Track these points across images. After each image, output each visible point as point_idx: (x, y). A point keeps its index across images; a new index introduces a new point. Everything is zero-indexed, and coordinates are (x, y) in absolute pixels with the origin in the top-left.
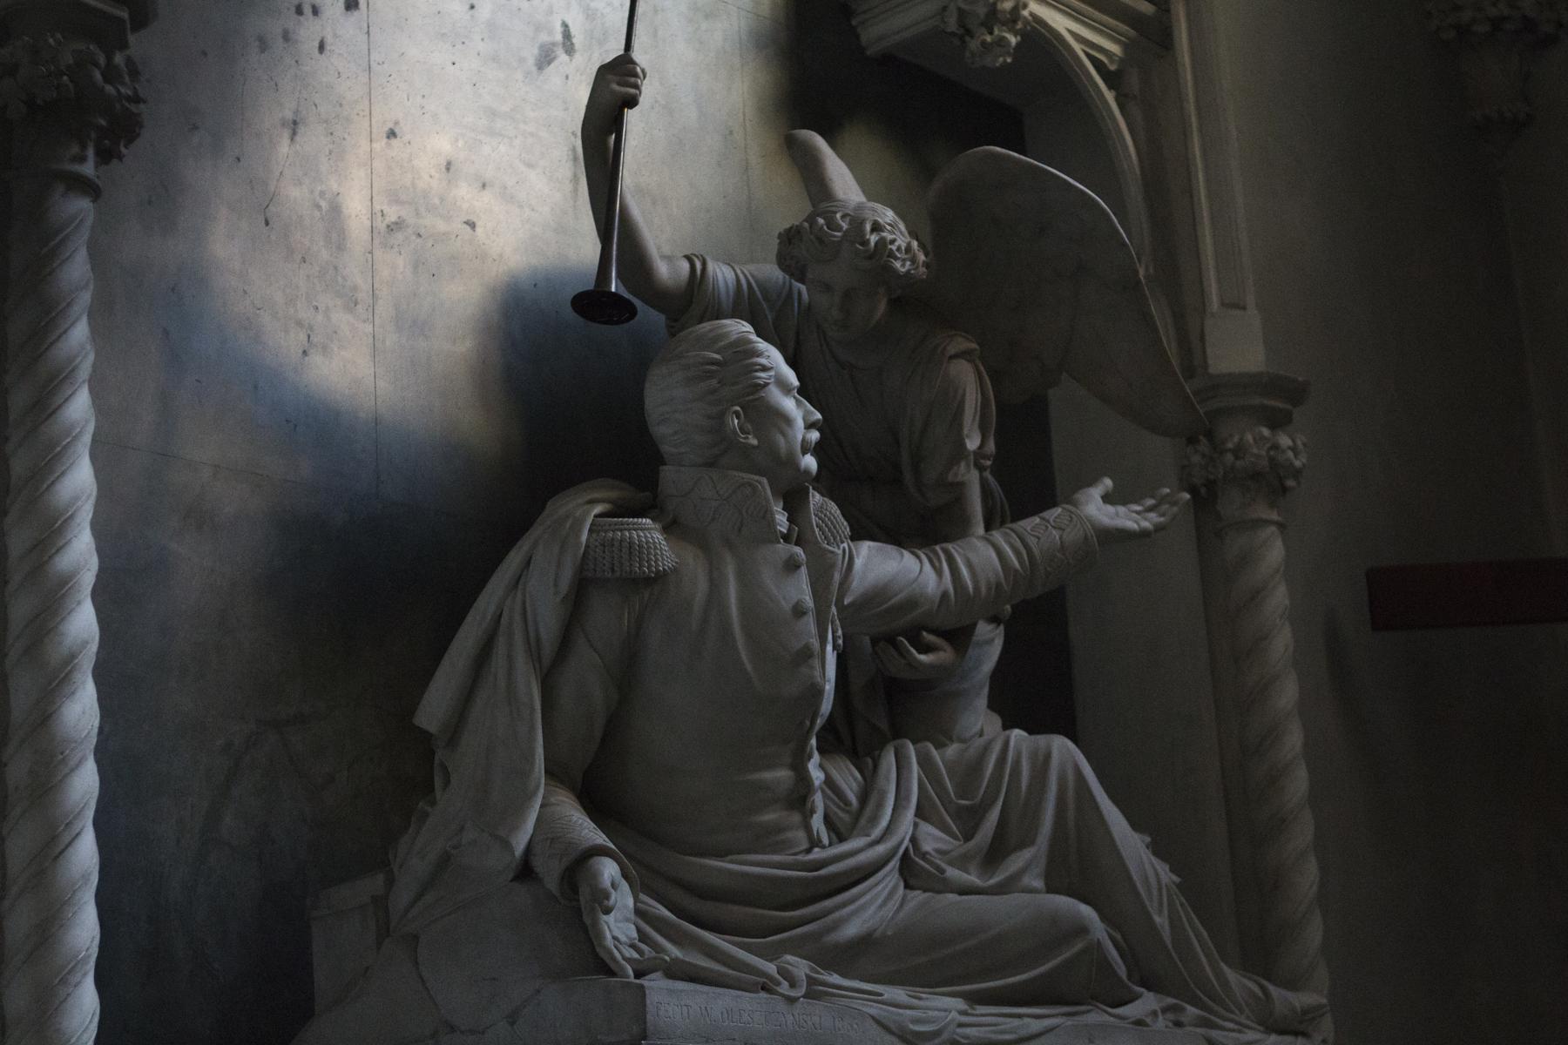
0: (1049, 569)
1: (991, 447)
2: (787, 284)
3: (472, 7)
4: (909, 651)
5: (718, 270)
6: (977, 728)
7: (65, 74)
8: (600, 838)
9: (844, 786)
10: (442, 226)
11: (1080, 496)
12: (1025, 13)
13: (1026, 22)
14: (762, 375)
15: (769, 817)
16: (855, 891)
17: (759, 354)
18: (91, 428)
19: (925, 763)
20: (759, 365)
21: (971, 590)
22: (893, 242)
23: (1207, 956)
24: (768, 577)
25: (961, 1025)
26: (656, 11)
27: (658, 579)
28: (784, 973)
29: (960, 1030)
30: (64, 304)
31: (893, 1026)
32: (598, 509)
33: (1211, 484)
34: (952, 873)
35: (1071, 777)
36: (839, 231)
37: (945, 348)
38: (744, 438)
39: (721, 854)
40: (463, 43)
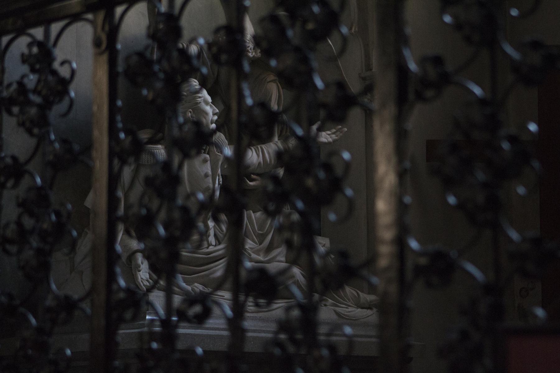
14: (199, 99)
20: (198, 96)
21: (268, 160)
37: (266, 79)
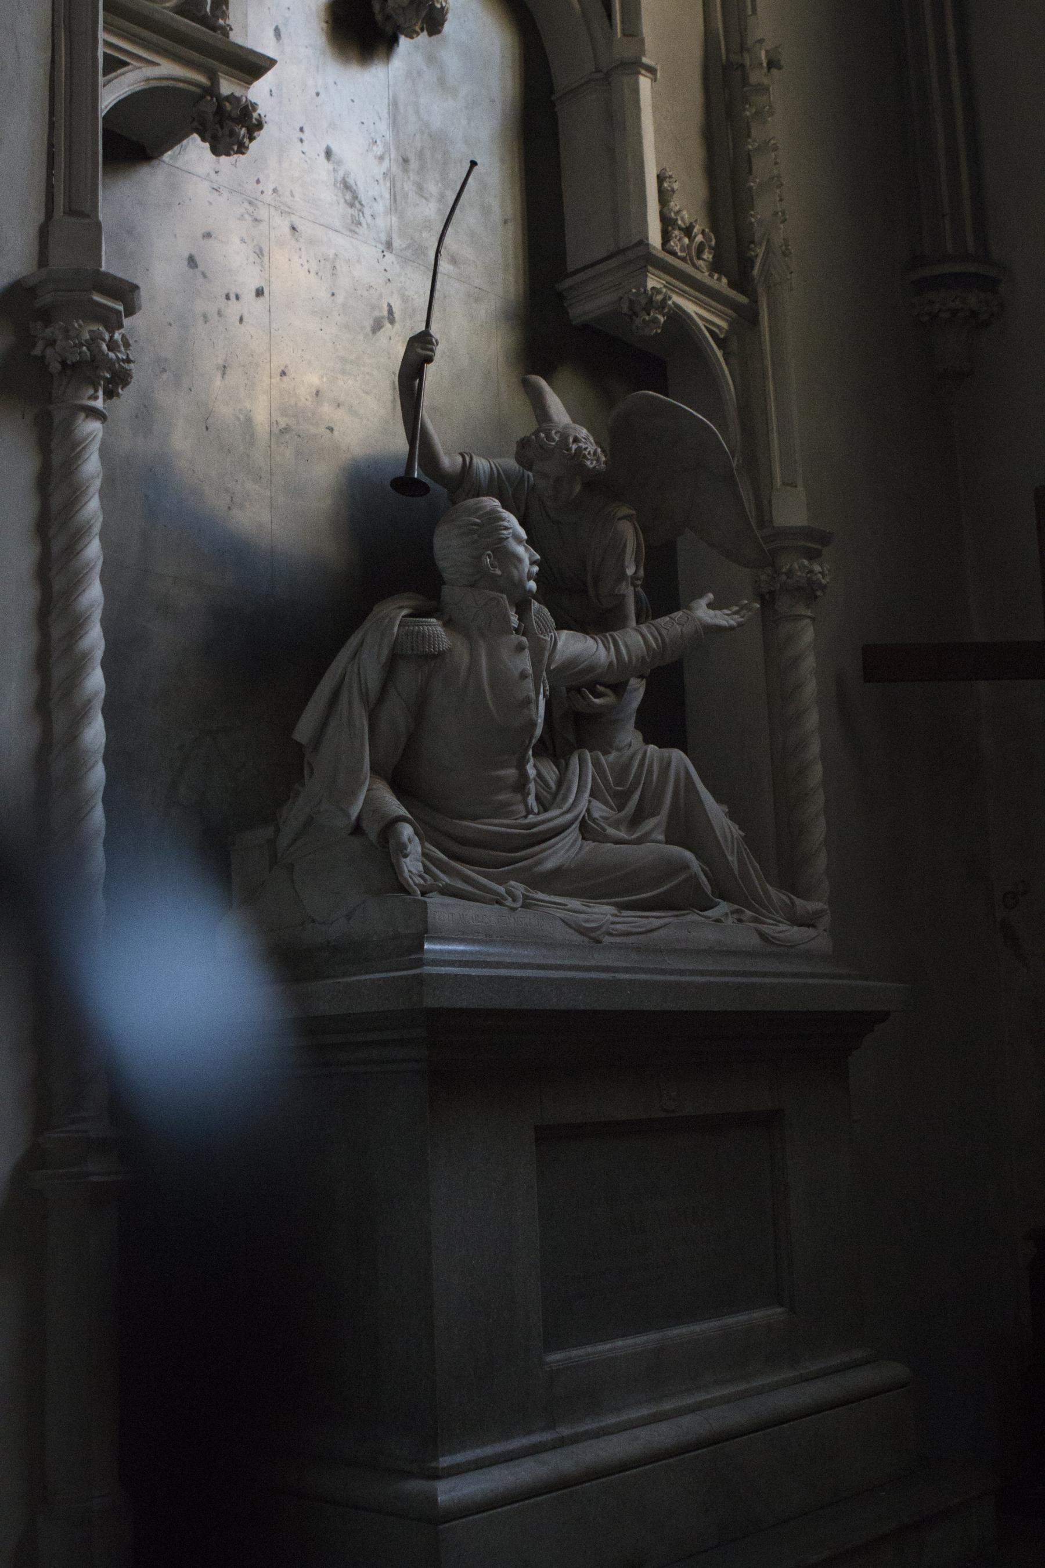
0: (673, 649)
1: (641, 573)
2: (521, 471)
3: (333, 294)
4: (588, 696)
5: (479, 462)
6: (627, 742)
7: (85, 346)
8: (403, 811)
9: (548, 777)
10: (313, 430)
11: (694, 604)
12: (670, 302)
13: (670, 308)
14: (505, 532)
15: (502, 797)
16: (553, 841)
17: (503, 520)
18: (100, 563)
19: (597, 764)
20: (504, 526)
21: (626, 659)
22: (586, 449)
23: (759, 880)
24: (505, 654)
25: (613, 923)
26: (445, 297)
27: (440, 656)
28: (509, 893)
29: (612, 926)
30: (85, 488)
31: (574, 925)
32: (405, 612)
33: (771, 593)
34: (611, 831)
35: (682, 775)
36: (552, 442)
37: (616, 513)
38: (493, 570)
39: (474, 818)
40: (327, 317)
